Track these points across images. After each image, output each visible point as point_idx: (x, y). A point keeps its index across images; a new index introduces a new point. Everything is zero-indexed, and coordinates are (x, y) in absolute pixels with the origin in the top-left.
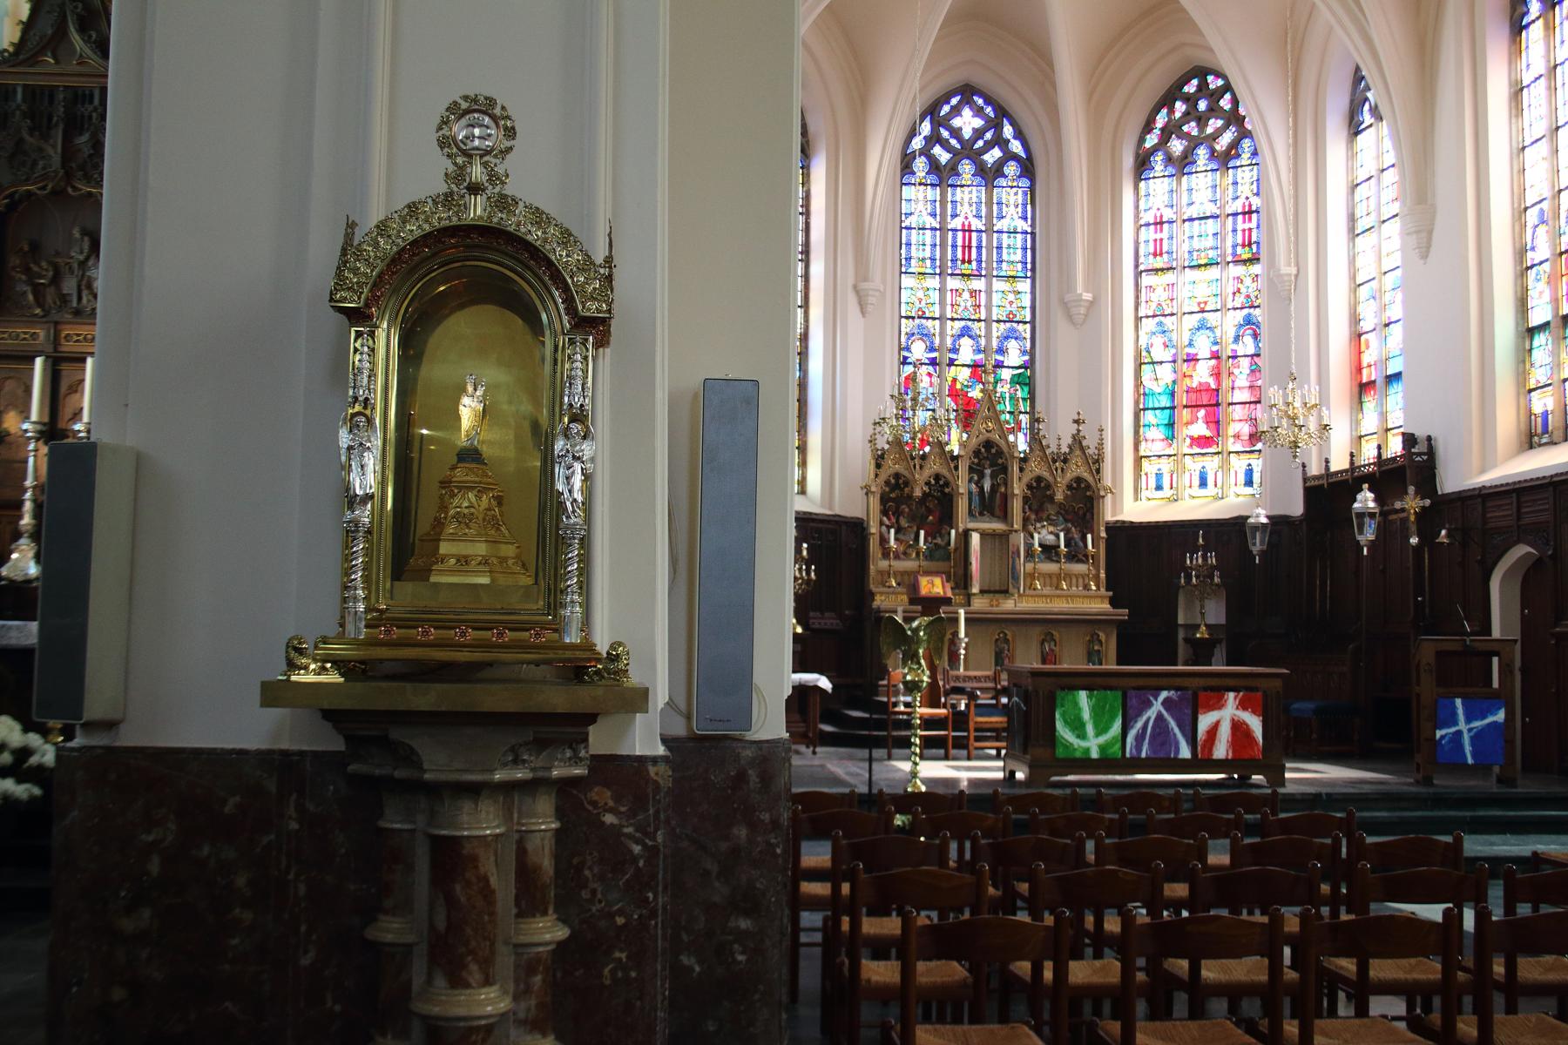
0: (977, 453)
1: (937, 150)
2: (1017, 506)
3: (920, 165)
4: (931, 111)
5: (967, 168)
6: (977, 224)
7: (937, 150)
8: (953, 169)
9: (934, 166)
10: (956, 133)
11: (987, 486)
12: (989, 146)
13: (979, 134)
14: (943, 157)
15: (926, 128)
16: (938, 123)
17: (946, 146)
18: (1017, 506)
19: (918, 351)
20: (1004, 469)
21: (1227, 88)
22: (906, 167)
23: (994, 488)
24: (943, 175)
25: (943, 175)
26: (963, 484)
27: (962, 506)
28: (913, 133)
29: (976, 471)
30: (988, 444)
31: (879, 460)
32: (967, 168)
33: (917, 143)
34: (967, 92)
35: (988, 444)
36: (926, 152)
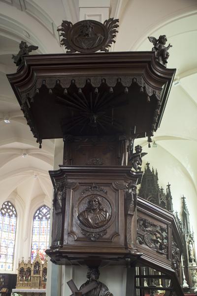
0: (35, 263)
1: (40, 215)
2: (41, 272)
3: (37, 218)
4: (39, 209)
5: (44, 218)
6: (45, 227)
7: (40, 215)
8: (42, 218)
9: (39, 218)
10: (42, 213)
11: (37, 269)
12: (48, 214)
13: (46, 213)
14: (40, 216)
15: (38, 212)
16: (40, 211)
17: (41, 214)
18: (41, 272)
19: (35, 247)
20: (39, 267)
21: (4, 204)
22: (34, 218)
23: (38, 269)
24: (41, 219)
25: (41, 219)
26: (32, 268)
27: (32, 272)
28: (36, 212)
29: (35, 267)
30: (37, 262)
31: (19, 264)
32: (44, 218)
33: (37, 214)
34: (45, 206)
35: (37, 262)
36: (38, 216)
